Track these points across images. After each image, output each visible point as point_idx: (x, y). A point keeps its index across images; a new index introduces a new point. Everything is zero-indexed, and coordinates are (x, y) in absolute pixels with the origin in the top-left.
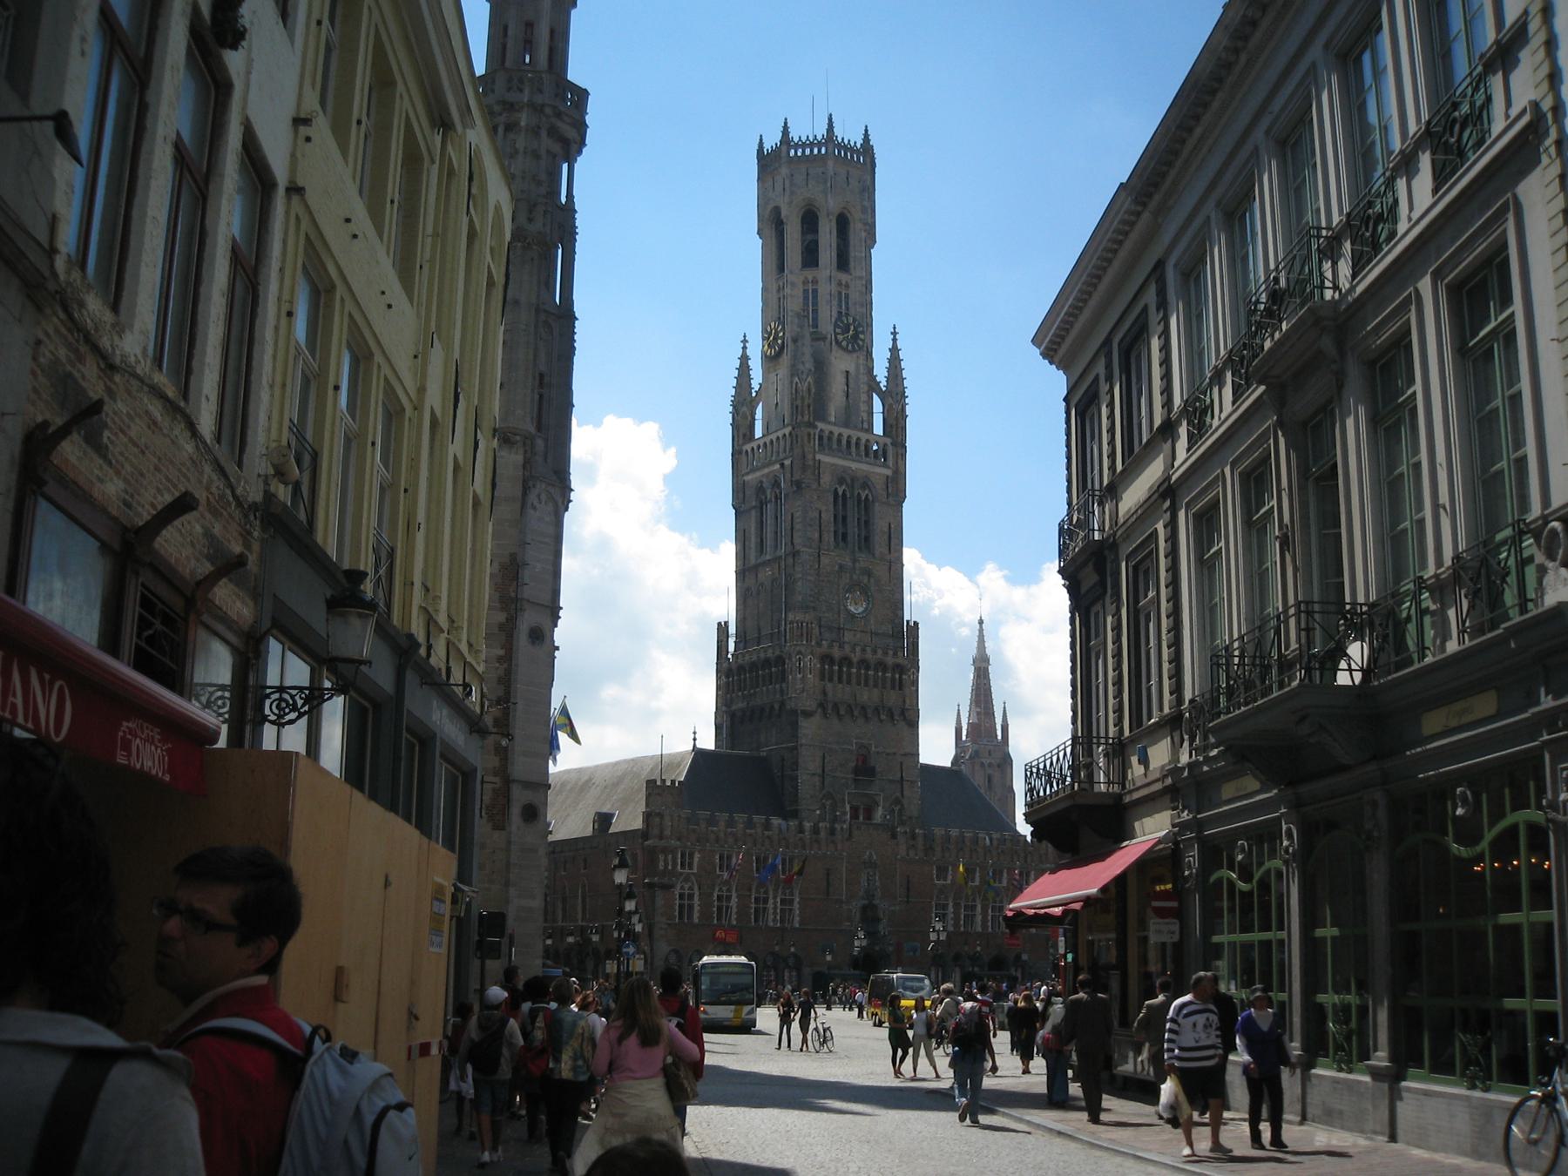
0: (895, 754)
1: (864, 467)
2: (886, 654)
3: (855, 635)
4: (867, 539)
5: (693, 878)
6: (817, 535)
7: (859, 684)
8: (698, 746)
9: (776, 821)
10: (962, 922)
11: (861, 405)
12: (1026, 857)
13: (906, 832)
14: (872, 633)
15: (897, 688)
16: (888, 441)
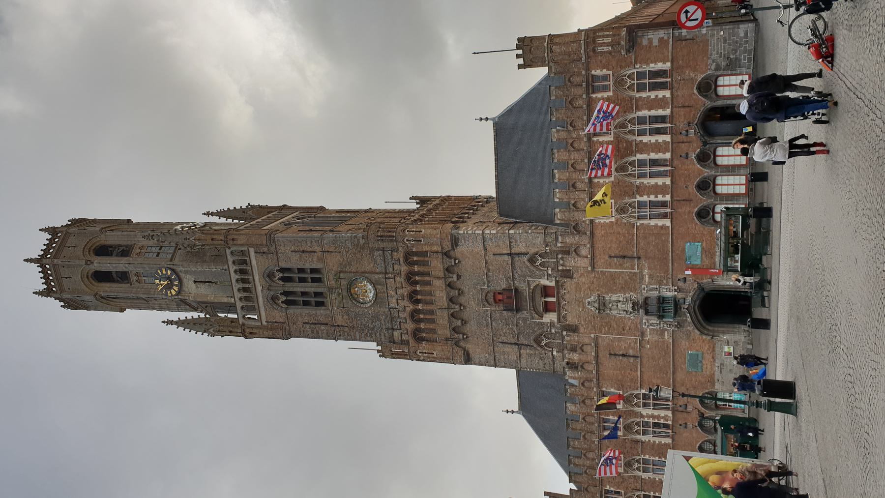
0: (486, 262)
1: (257, 278)
2: (399, 274)
3: (392, 297)
4: (313, 271)
5: (629, 494)
6: (323, 327)
7: (431, 303)
8: (518, 410)
9: (571, 407)
10: (660, 181)
11: (213, 270)
12: (576, 85)
13: (562, 258)
14: (386, 278)
15: (426, 259)
16: (228, 251)
